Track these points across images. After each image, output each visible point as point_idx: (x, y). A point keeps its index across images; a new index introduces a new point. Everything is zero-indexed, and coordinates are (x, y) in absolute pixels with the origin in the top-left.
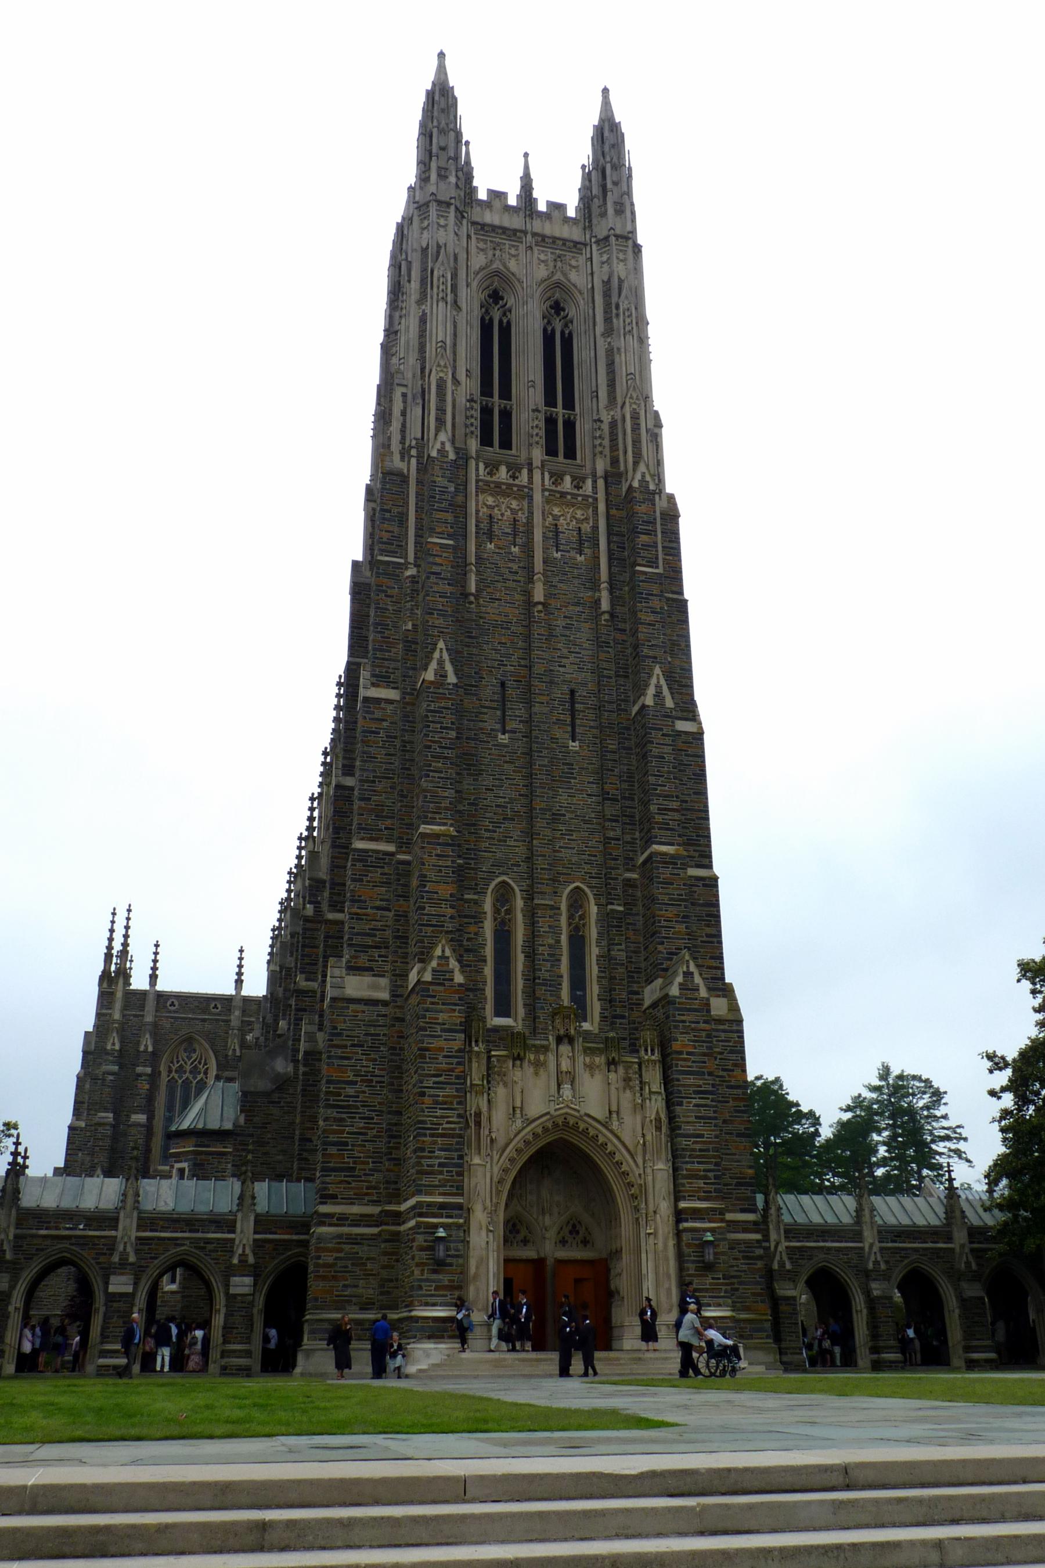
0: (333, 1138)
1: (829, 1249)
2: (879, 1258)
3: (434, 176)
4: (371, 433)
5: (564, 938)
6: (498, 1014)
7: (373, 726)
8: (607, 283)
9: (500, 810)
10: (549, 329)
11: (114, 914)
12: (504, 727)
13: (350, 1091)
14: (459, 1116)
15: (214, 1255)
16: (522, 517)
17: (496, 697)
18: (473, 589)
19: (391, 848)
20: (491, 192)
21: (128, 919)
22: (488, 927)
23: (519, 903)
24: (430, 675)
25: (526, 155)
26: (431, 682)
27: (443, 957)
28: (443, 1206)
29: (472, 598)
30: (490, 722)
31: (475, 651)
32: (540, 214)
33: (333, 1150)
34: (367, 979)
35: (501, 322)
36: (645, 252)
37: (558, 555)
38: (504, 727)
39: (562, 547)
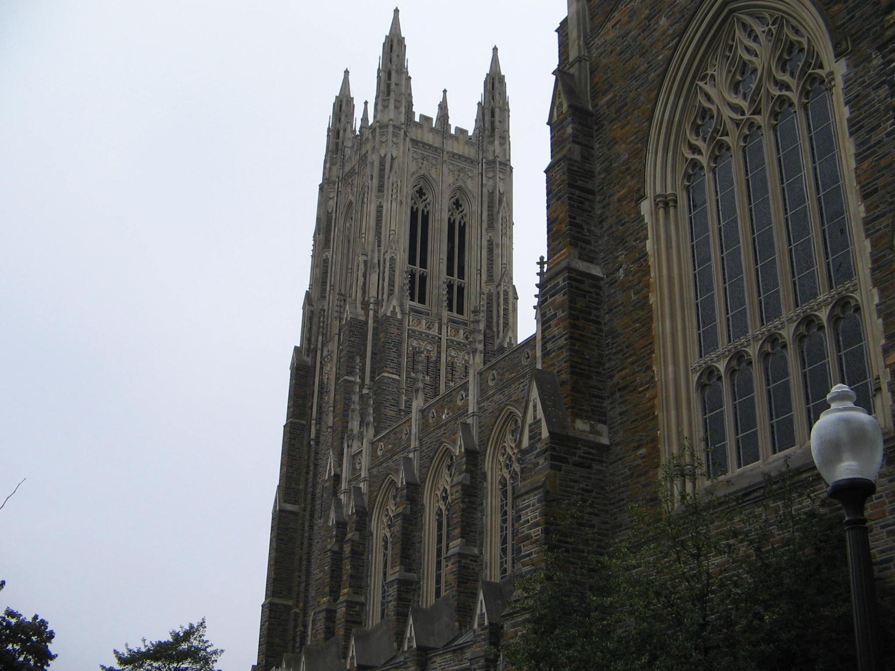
3: (392, 106)
4: (311, 253)
8: (491, 194)
10: (452, 220)
20: (422, 116)
25: (445, 91)
32: (451, 136)
35: (423, 211)
36: (514, 170)
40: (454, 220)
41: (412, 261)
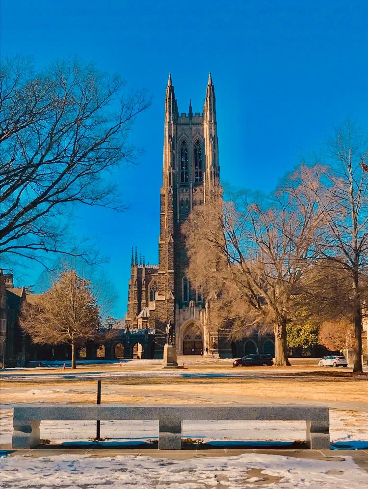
6: (185, 300)
11: (133, 248)
16: (189, 199)
20: (182, 114)
22: (183, 287)
25: (190, 100)
34: (161, 296)
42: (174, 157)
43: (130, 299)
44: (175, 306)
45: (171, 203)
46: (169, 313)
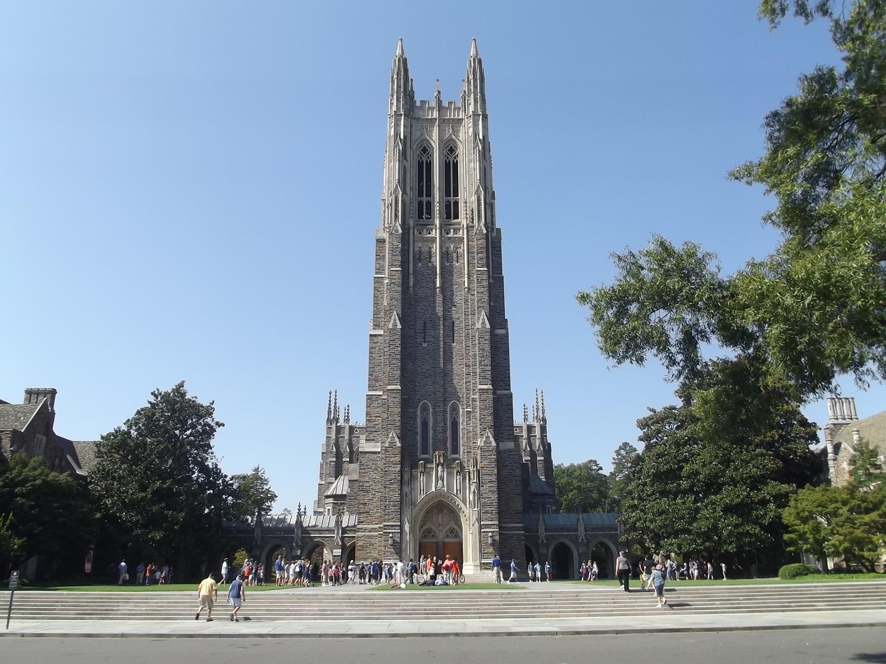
0: (362, 502)
1: (564, 535)
2: (584, 537)
5: (449, 423)
7: (374, 345)
9: (423, 374)
11: (330, 393)
12: (425, 340)
13: (367, 484)
14: (399, 494)
15: (328, 542)
17: (422, 328)
18: (411, 284)
19: (381, 393)
21: (336, 396)
23: (431, 410)
24: (390, 326)
26: (391, 329)
27: (392, 437)
28: (392, 526)
29: (411, 289)
30: (420, 340)
31: (413, 311)
33: (361, 506)
34: (372, 444)
35: (427, 161)
37: (448, 264)
38: (425, 340)
39: (449, 261)
40: (449, 161)
41: (420, 194)
42: (405, 173)
43: (324, 476)
44: (402, 463)
45: (397, 253)
46: (389, 478)
